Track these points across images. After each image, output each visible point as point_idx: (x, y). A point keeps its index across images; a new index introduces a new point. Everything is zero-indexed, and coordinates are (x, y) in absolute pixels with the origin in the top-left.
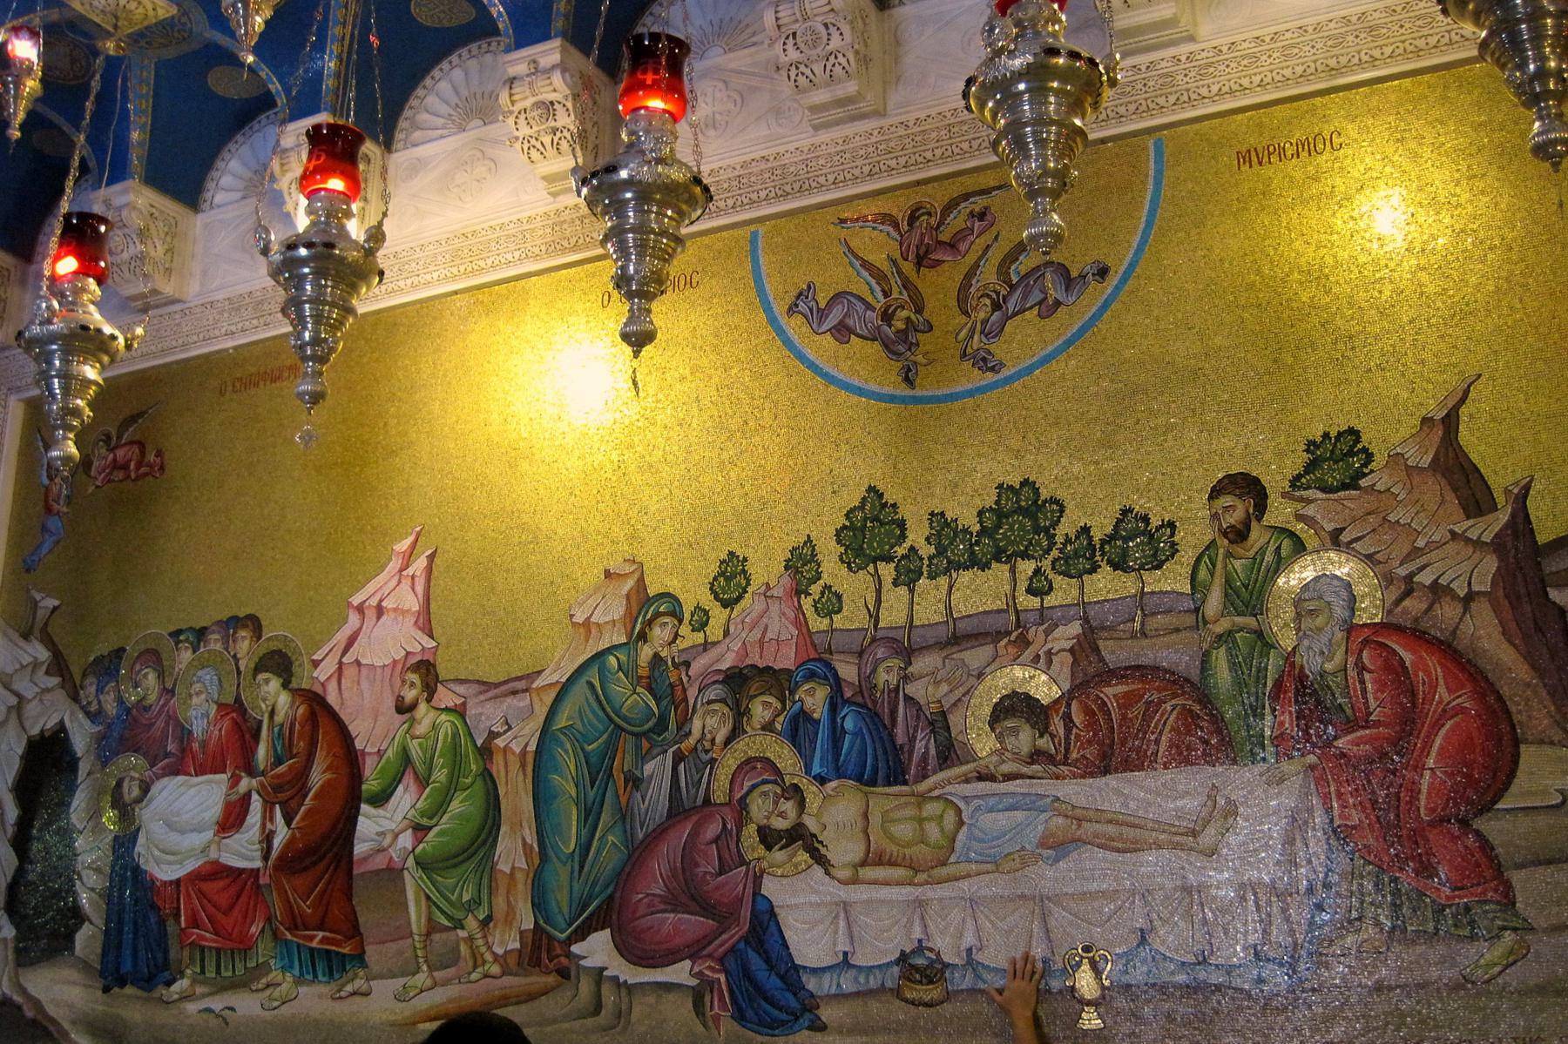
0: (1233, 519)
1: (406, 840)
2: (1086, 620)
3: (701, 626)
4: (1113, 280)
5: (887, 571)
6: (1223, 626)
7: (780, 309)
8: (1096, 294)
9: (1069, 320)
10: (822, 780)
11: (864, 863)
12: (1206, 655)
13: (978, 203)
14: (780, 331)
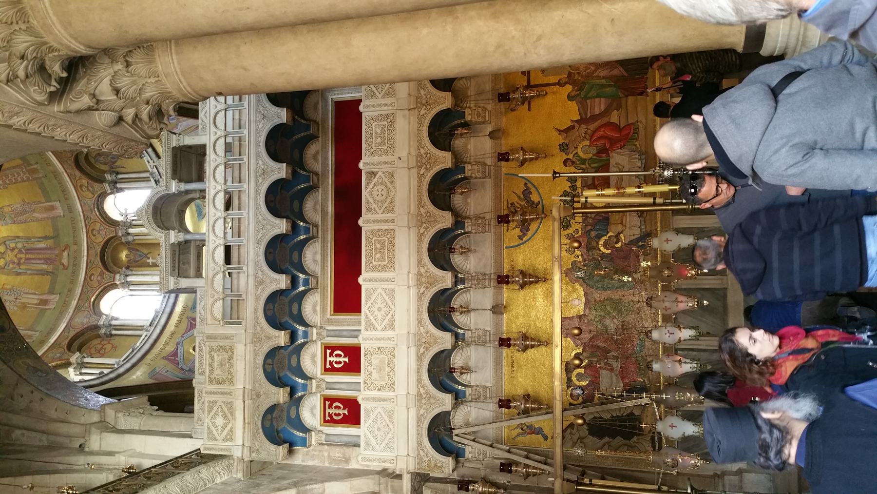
0: (570, 163)
1: (615, 321)
2: (584, 187)
3: (578, 256)
4: (527, 182)
5: (572, 221)
6: (587, 165)
7: (521, 242)
8: (529, 185)
9: (532, 189)
10: (608, 233)
11: (623, 224)
12: (592, 168)
13: (510, 205)
14: (525, 242)
